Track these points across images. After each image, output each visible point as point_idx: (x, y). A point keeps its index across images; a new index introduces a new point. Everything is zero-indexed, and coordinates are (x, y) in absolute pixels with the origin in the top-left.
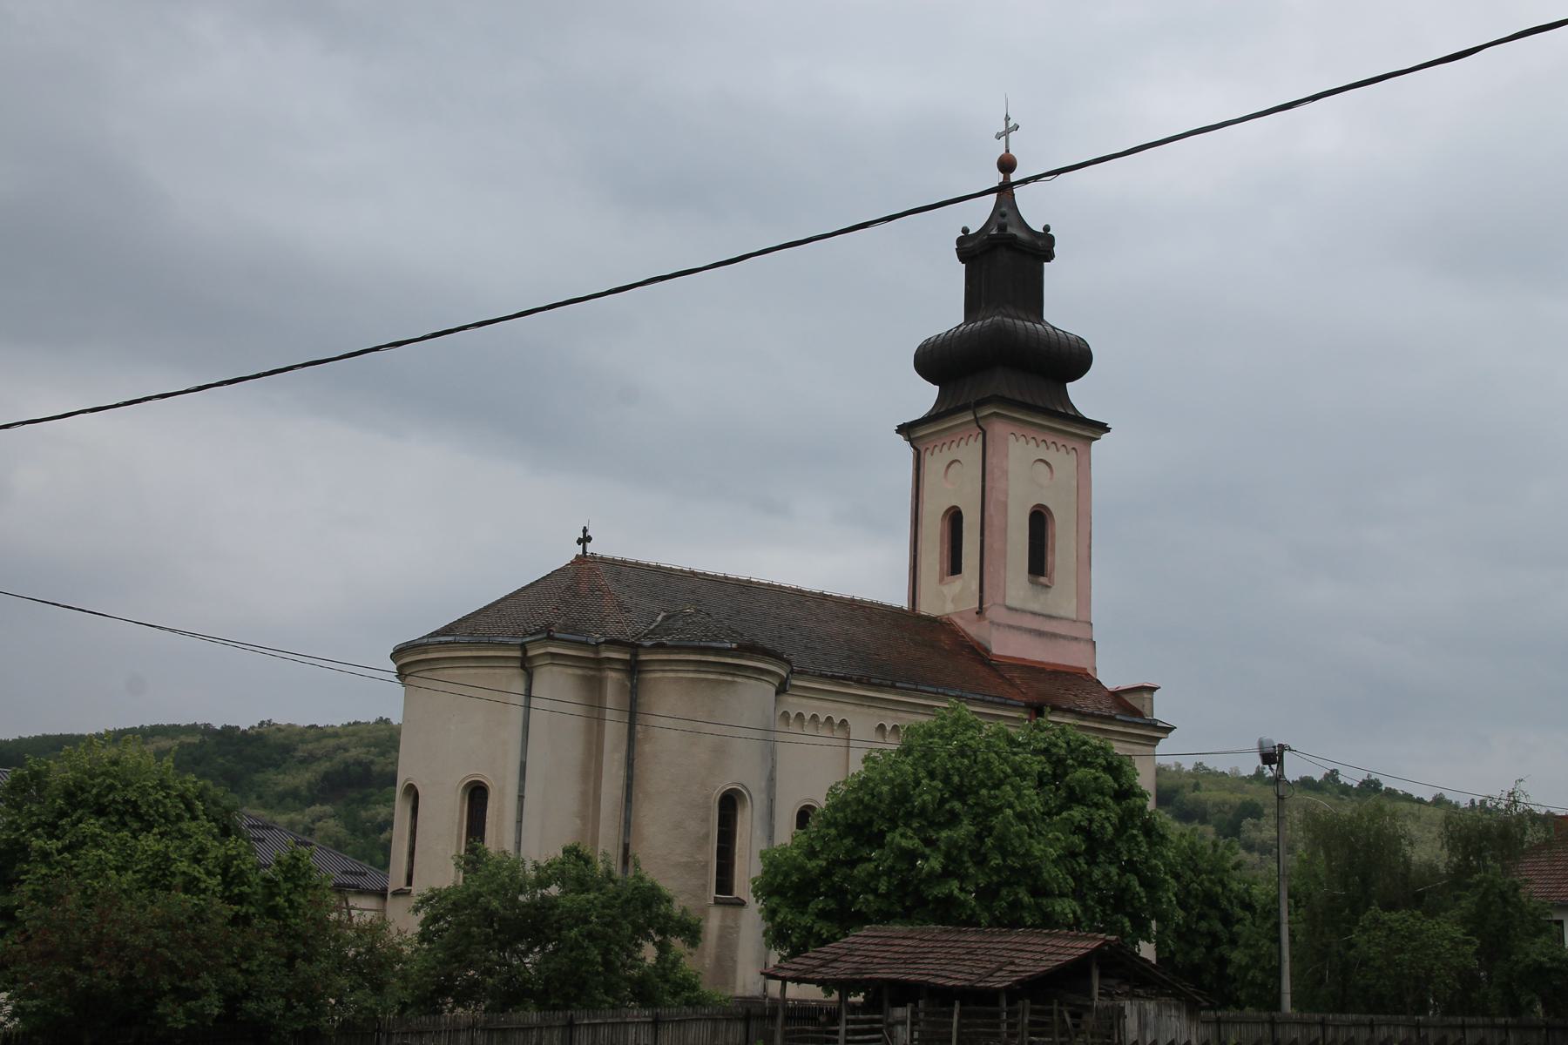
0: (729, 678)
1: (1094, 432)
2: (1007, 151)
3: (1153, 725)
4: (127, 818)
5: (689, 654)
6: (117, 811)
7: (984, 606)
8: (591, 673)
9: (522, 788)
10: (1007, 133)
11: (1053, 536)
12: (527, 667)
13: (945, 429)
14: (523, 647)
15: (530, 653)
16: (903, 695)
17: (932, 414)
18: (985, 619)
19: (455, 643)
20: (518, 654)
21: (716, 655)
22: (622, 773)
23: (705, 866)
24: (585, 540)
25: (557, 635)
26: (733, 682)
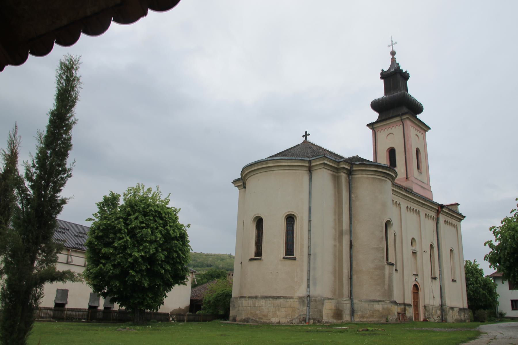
0: (384, 179)
1: (427, 129)
2: (393, 50)
3: (460, 215)
4: (156, 219)
5: (373, 167)
6: (152, 214)
7: (408, 176)
8: (335, 174)
9: (310, 217)
10: (392, 45)
11: (421, 158)
12: (310, 170)
14: (310, 162)
15: (312, 164)
17: (379, 120)
18: (409, 180)
20: (307, 165)
23: (383, 249)
24: (306, 135)
25: (327, 156)
26: (386, 180)
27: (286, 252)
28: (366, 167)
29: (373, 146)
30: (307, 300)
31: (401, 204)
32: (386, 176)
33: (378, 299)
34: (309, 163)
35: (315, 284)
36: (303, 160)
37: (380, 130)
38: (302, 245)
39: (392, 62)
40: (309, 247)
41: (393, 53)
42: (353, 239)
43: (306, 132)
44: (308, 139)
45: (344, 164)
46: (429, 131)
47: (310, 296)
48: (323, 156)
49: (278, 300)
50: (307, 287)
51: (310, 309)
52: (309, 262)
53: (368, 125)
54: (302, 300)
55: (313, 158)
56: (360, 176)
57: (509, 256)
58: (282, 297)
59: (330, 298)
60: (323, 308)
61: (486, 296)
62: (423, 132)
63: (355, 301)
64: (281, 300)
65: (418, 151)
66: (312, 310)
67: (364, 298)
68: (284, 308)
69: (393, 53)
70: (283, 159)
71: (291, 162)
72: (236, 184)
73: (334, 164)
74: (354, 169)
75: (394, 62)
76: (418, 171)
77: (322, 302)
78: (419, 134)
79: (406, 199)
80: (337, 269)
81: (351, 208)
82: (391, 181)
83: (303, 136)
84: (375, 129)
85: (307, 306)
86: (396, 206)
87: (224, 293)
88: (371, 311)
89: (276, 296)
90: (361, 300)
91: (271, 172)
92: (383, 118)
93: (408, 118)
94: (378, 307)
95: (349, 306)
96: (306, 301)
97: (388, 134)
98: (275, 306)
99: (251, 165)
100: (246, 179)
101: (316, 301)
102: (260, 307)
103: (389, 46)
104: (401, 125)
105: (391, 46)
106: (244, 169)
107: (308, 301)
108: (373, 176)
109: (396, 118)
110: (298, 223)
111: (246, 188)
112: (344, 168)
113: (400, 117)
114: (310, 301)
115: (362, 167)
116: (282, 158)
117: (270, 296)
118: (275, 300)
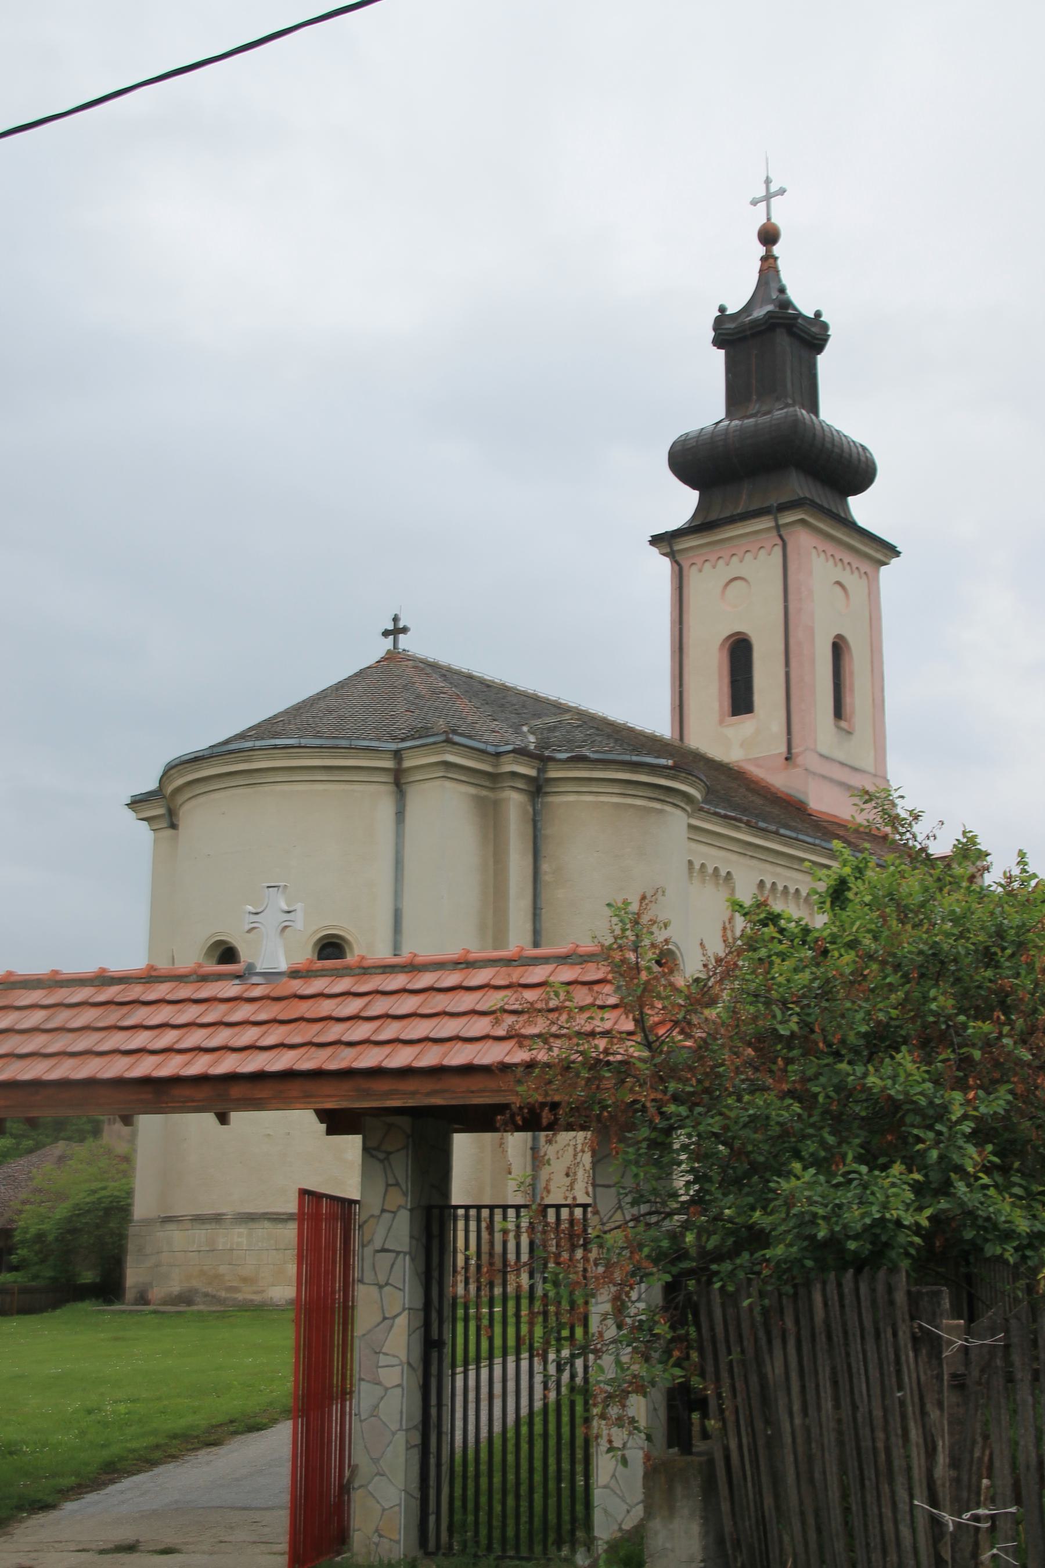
0: (657, 805)
1: (886, 555)
2: (769, 219)
5: (617, 770)
7: (794, 751)
8: (484, 793)
10: (768, 197)
11: (852, 673)
14: (397, 755)
15: (407, 764)
16: (785, 845)
18: (795, 766)
20: (389, 764)
21: (648, 774)
22: (529, 926)
28: (592, 770)
31: (735, 877)
32: (662, 797)
37: (699, 561)
39: (761, 271)
41: (769, 236)
43: (396, 619)
46: (894, 561)
48: (442, 738)
53: (656, 540)
56: (571, 798)
62: (866, 567)
65: (839, 648)
69: (769, 236)
73: (483, 761)
74: (552, 774)
75: (772, 272)
76: (838, 727)
78: (850, 579)
79: (755, 855)
81: (538, 912)
82: (683, 809)
83: (386, 633)
84: (678, 558)
86: (717, 884)
91: (267, 788)
93: (802, 522)
97: (727, 580)
99: (196, 760)
100: (180, 802)
103: (754, 203)
106: (172, 772)
109: (753, 521)
111: (180, 828)
112: (514, 774)
113: (771, 517)
115: (579, 769)
116: (303, 742)
117: (267, 1214)
118: (280, 1226)
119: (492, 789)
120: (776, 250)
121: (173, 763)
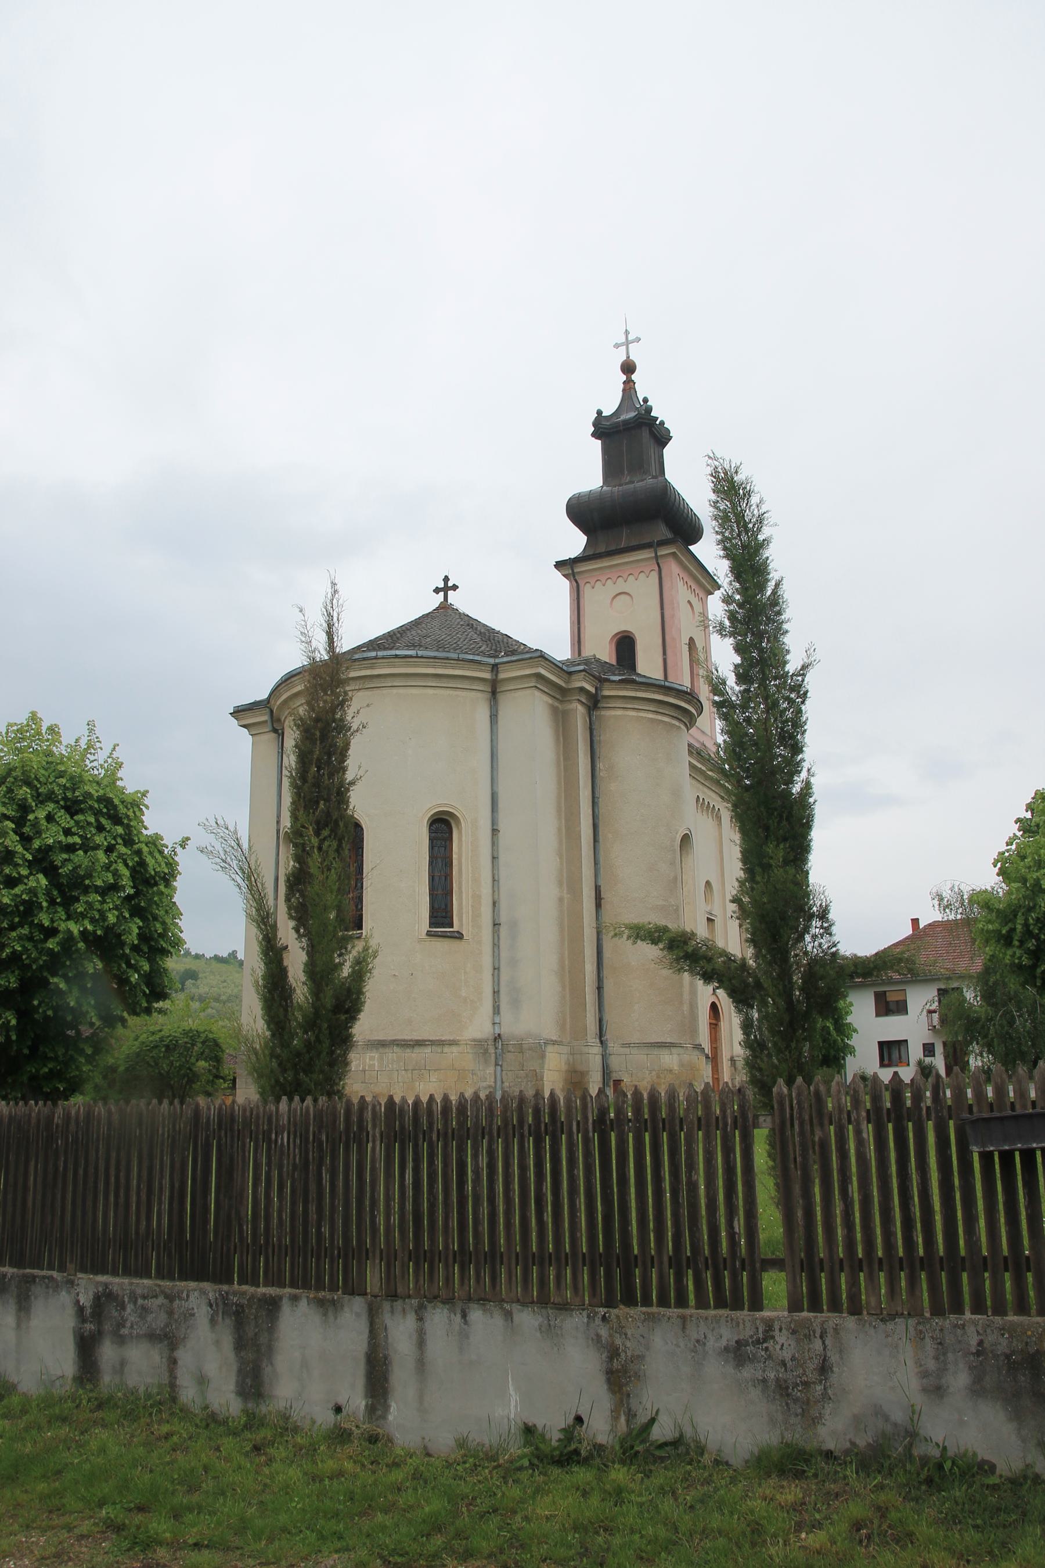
0: (677, 723)
1: (712, 587)
4: (103, 821)
5: (654, 692)
6: (91, 808)
8: (556, 704)
9: (494, 822)
10: (627, 343)
12: (494, 690)
13: (627, 563)
14: (495, 668)
19: (417, 657)
20: (487, 675)
21: (675, 697)
27: (431, 917)
28: (636, 690)
29: (572, 623)
30: (496, 1048)
32: (680, 717)
33: (669, 1040)
34: (492, 671)
35: (516, 1003)
36: (479, 662)
37: (592, 581)
38: (477, 898)
39: (624, 390)
40: (494, 903)
41: (628, 368)
42: (601, 882)
43: (446, 579)
44: (450, 601)
45: (584, 679)
47: (503, 1037)
49: (417, 1050)
50: (494, 1014)
51: (504, 1072)
52: (496, 945)
53: (559, 565)
54: (479, 1044)
55: (505, 659)
56: (619, 712)
57: (1040, 925)
58: (429, 1041)
59: (556, 1041)
60: (543, 1068)
61: (829, 1033)
63: (613, 1047)
64: (428, 1050)
66: (510, 1073)
67: (635, 1038)
68: (435, 1070)
69: (628, 368)
70: (422, 657)
71: (446, 667)
72: (243, 718)
74: (606, 693)
77: (539, 1049)
78: (695, 601)
80: (567, 963)
83: (437, 590)
85: (496, 1064)
87: (162, 1040)
88: (654, 1073)
89: (411, 1040)
90: (628, 1045)
91: (385, 691)
92: (602, 549)
93: (674, 554)
94: (670, 1060)
95: (598, 1059)
96: (492, 1050)
98: (410, 1068)
101: (520, 1048)
102: (364, 1071)
103: (617, 346)
104: (652, 572)
105: (624, 347)
106: (293, 679)
107: (499, 1051)
108: (666, 719)
110: (464, 838)
114: (502, 1049)
115: (627, 689)
116: (420, 653)
117: (395, 1040)
118: (408, 1050)
119: (561, 702)
120: (634, 377)
121: (294, 673)
